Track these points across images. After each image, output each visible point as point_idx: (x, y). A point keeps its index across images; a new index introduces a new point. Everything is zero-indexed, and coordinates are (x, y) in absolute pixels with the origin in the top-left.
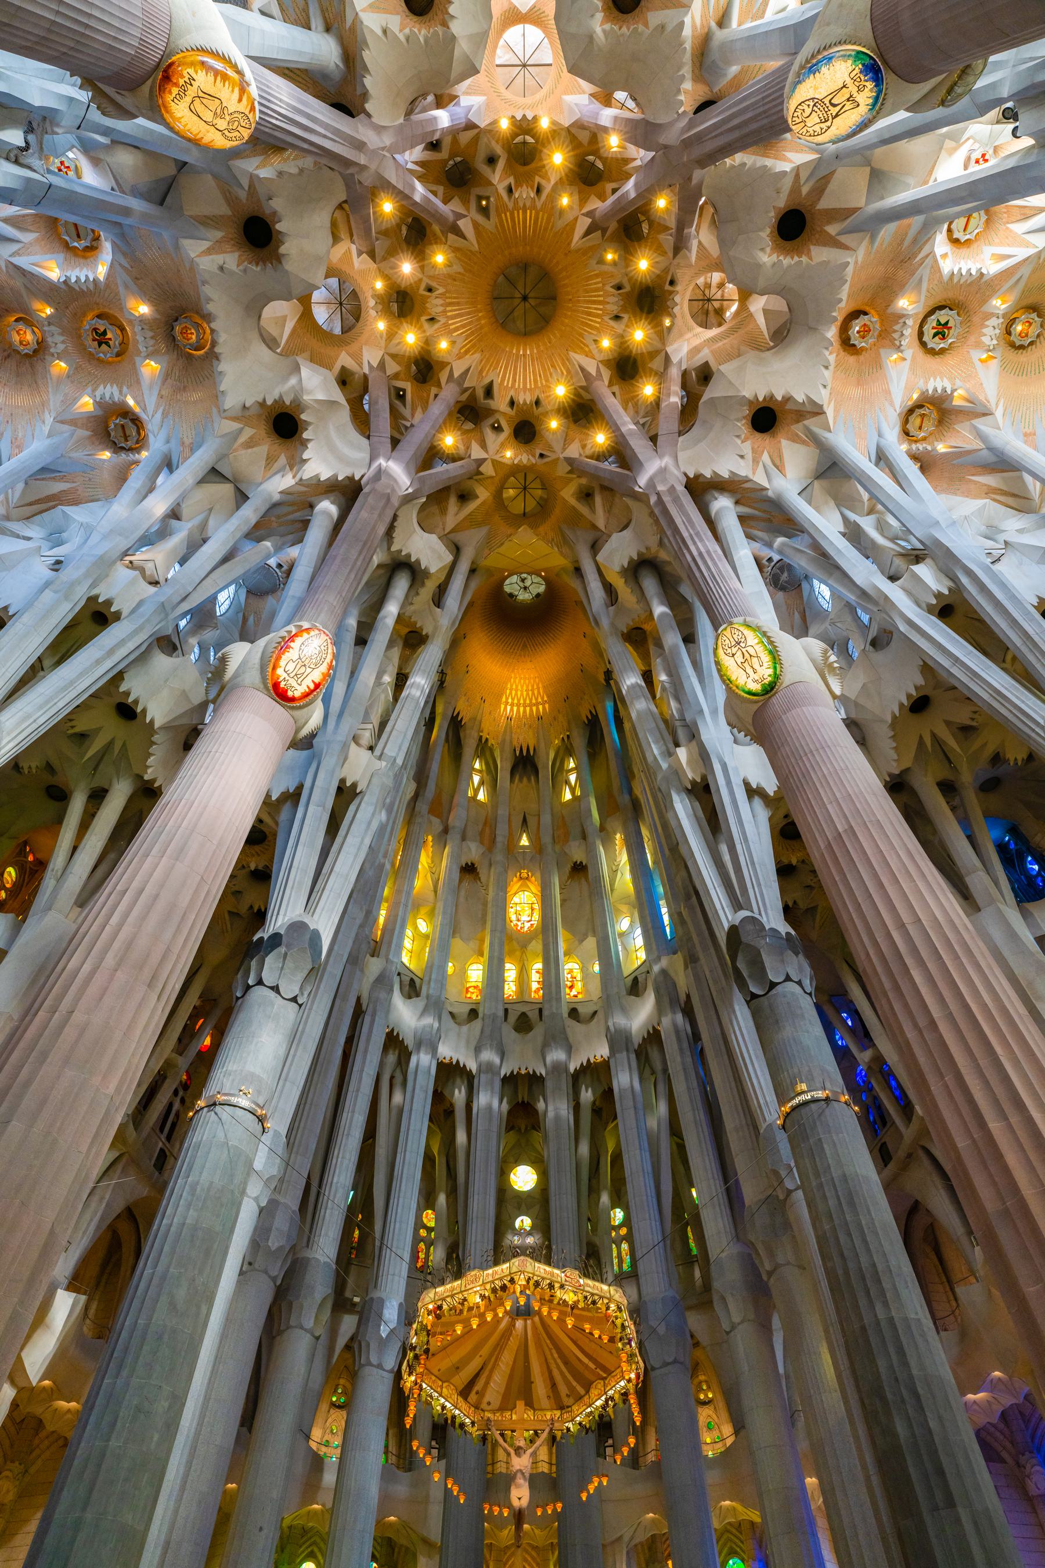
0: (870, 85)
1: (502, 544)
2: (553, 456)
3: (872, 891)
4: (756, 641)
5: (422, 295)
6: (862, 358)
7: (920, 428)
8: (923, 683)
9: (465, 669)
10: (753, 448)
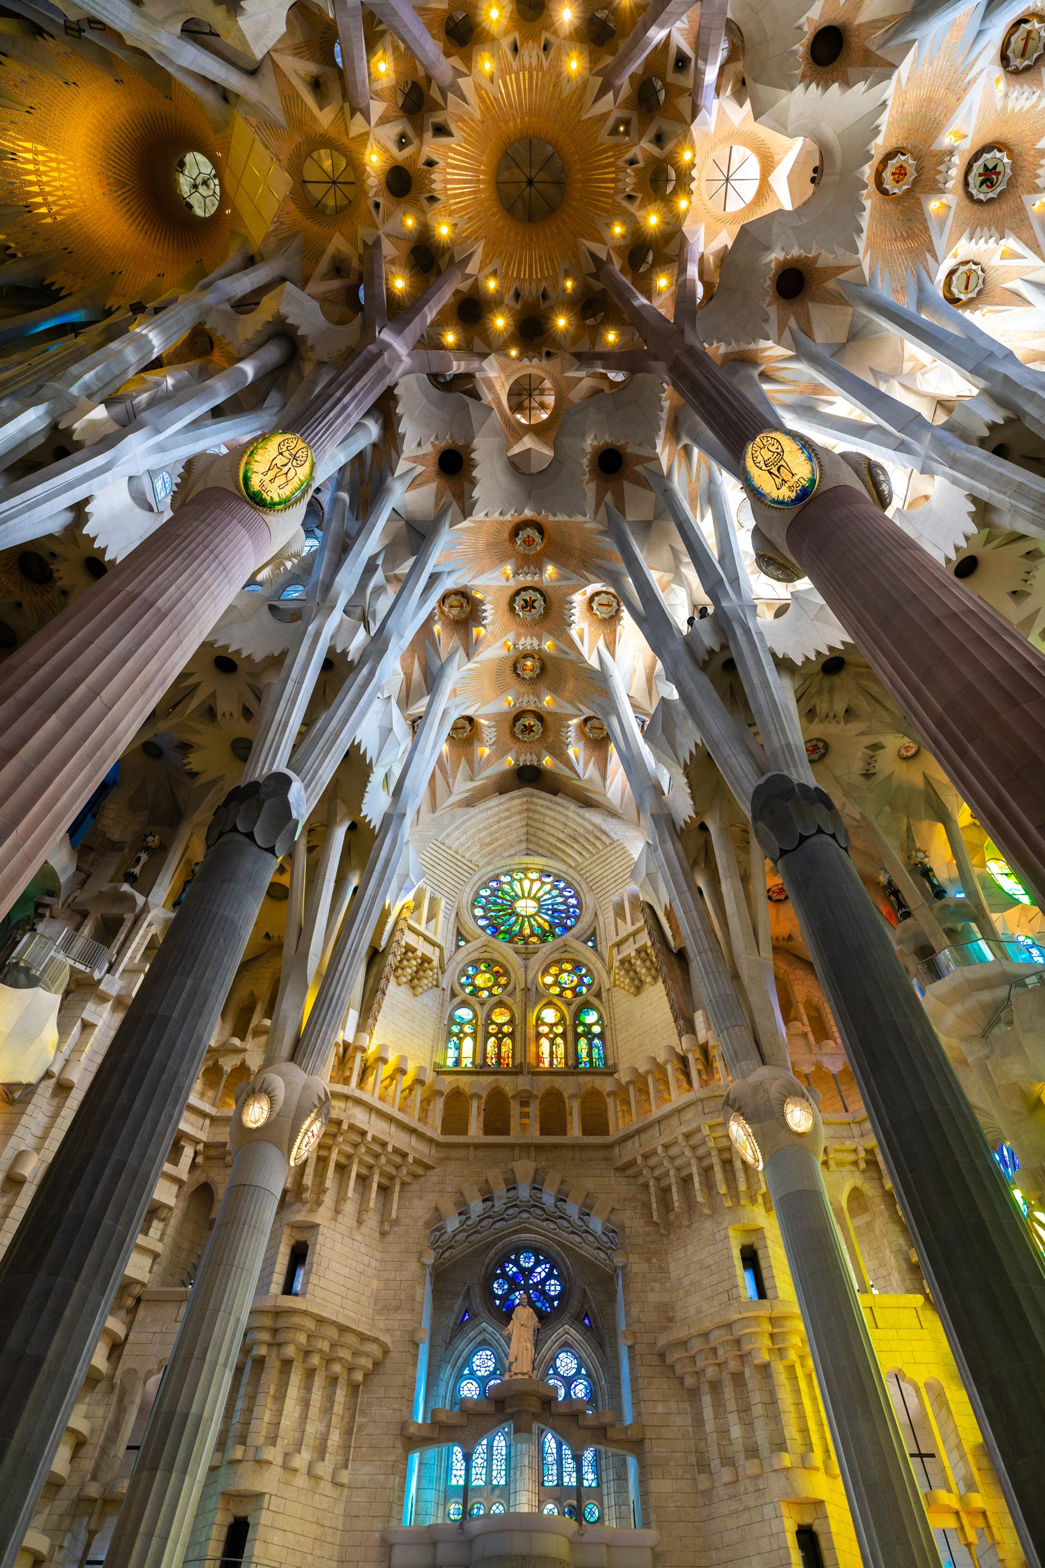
0: (793, 495)
1: (266, 146)
2: (379, 220)
3: (114, 652)
4: (302, 478)
5: (540, 35)
6: (507, 544)
7: (451, 606)
8: (257, 661)
9: (70, 80)
10: (426, 454)
